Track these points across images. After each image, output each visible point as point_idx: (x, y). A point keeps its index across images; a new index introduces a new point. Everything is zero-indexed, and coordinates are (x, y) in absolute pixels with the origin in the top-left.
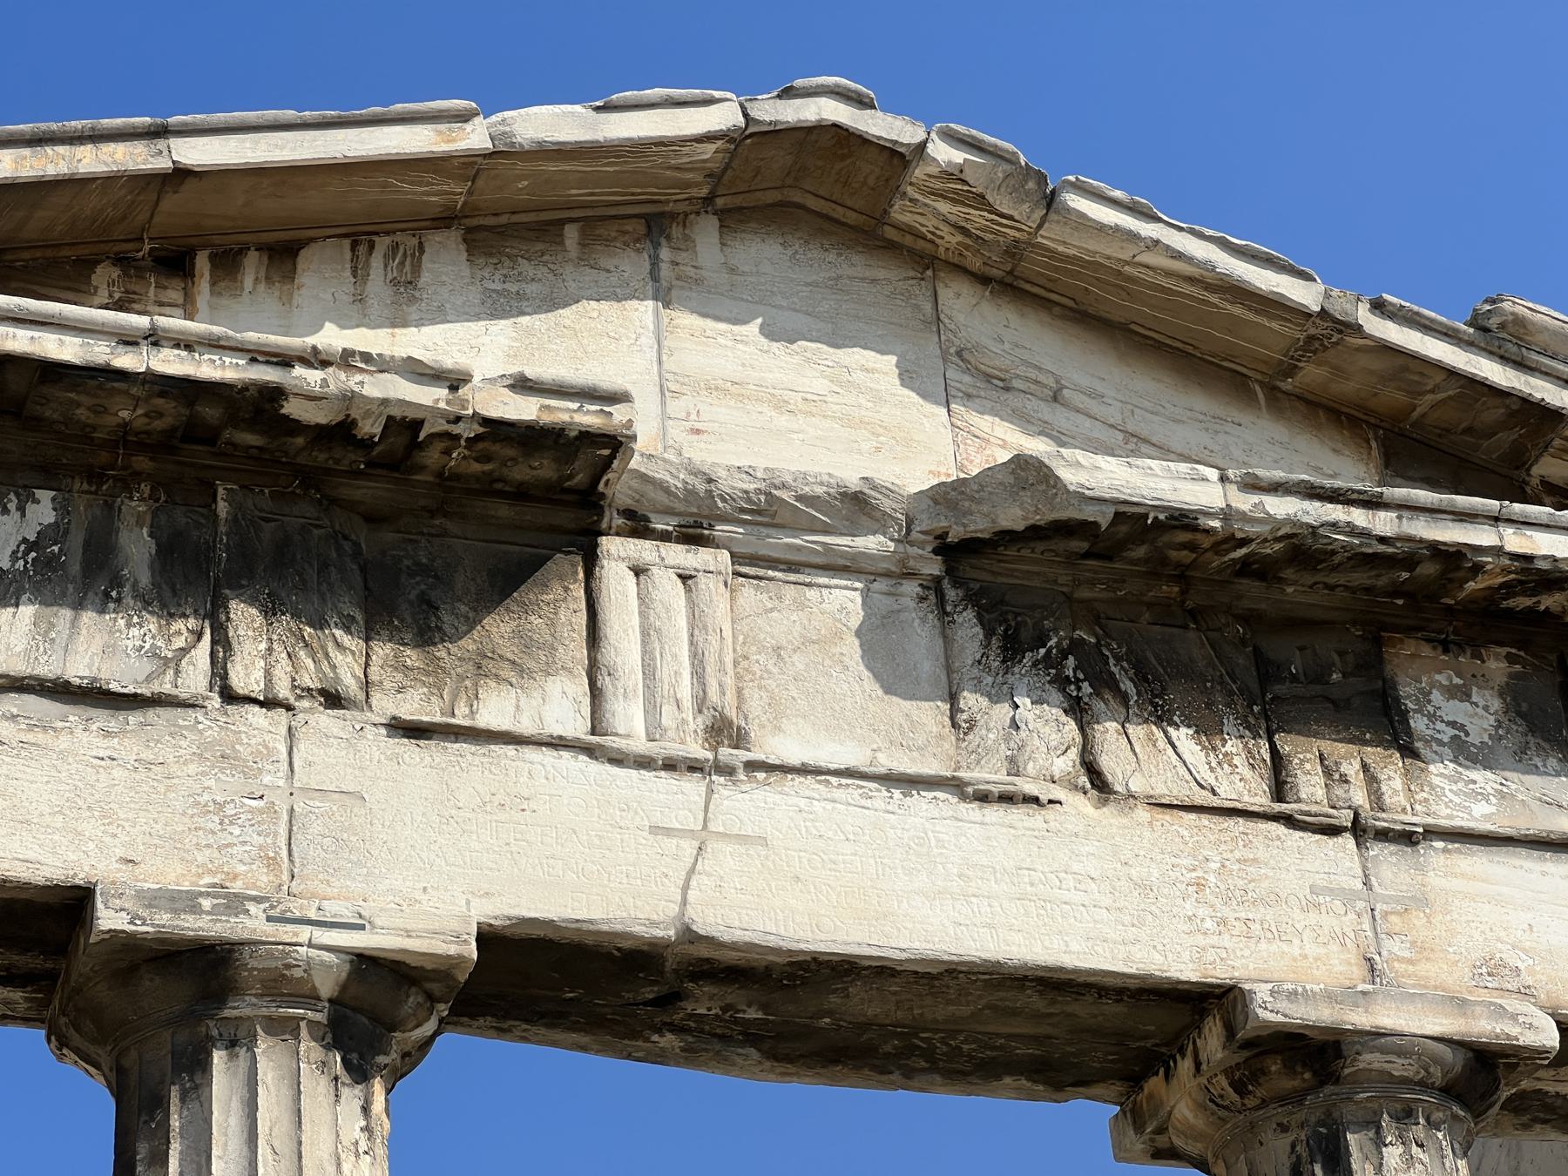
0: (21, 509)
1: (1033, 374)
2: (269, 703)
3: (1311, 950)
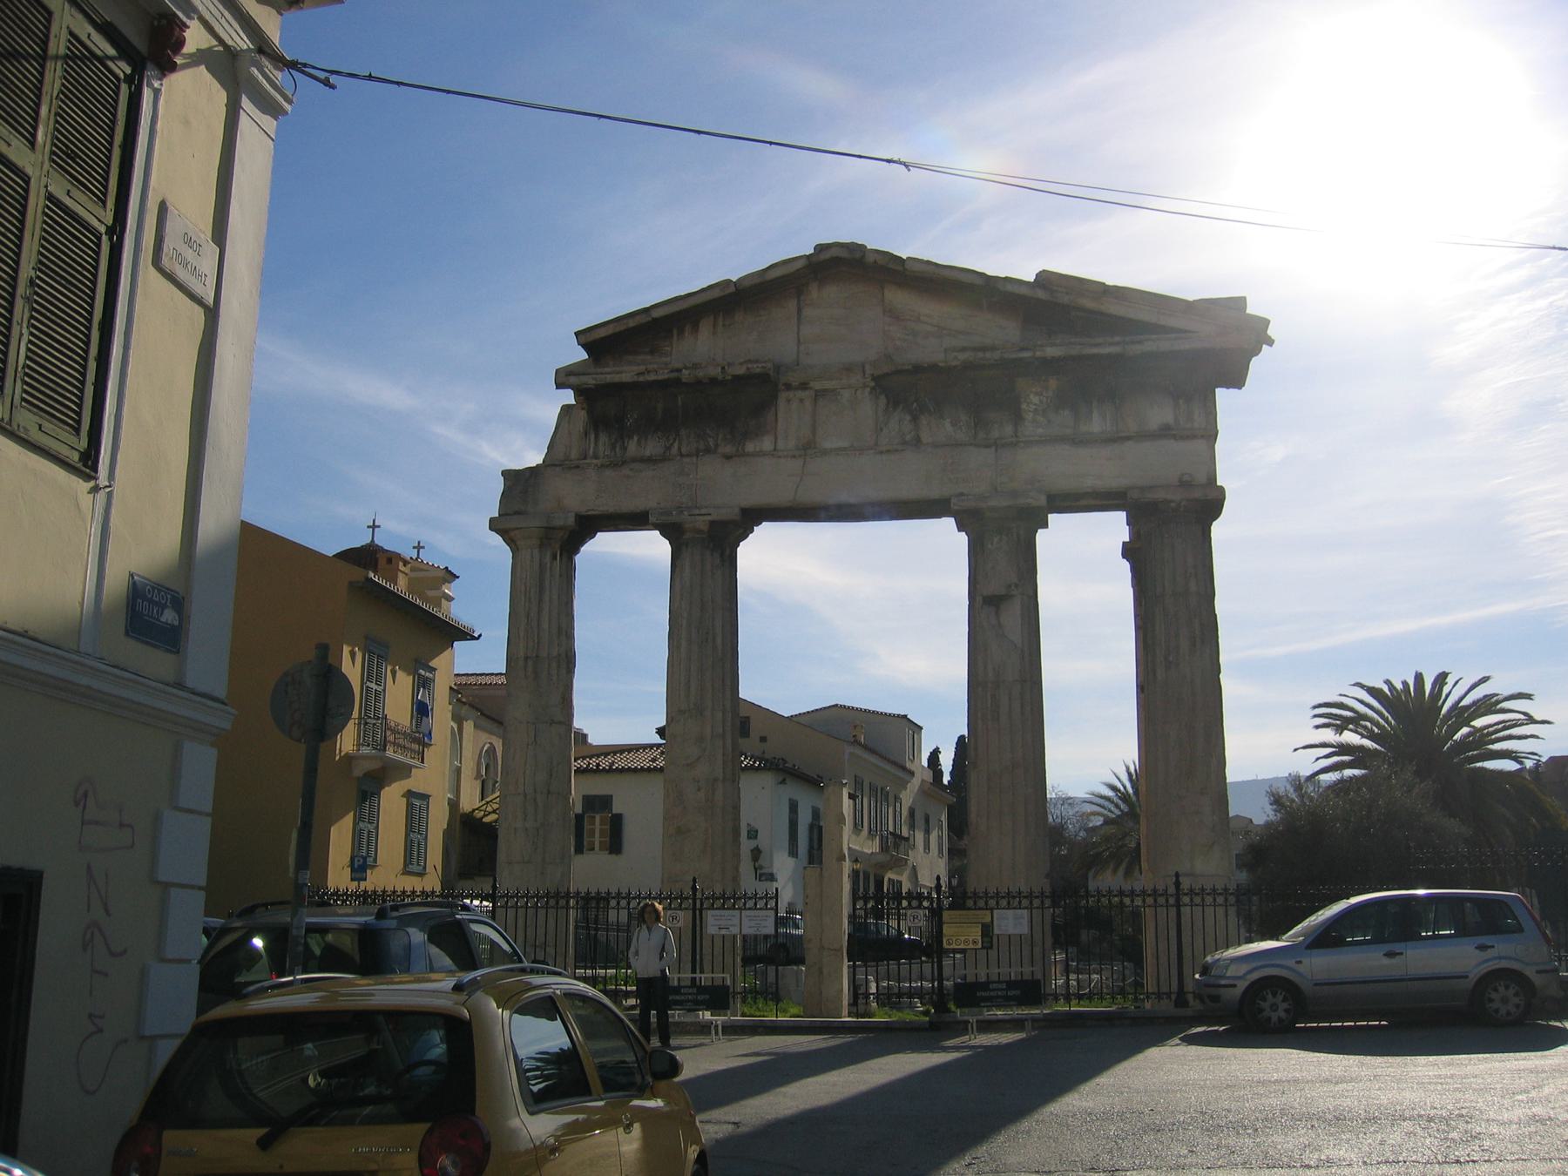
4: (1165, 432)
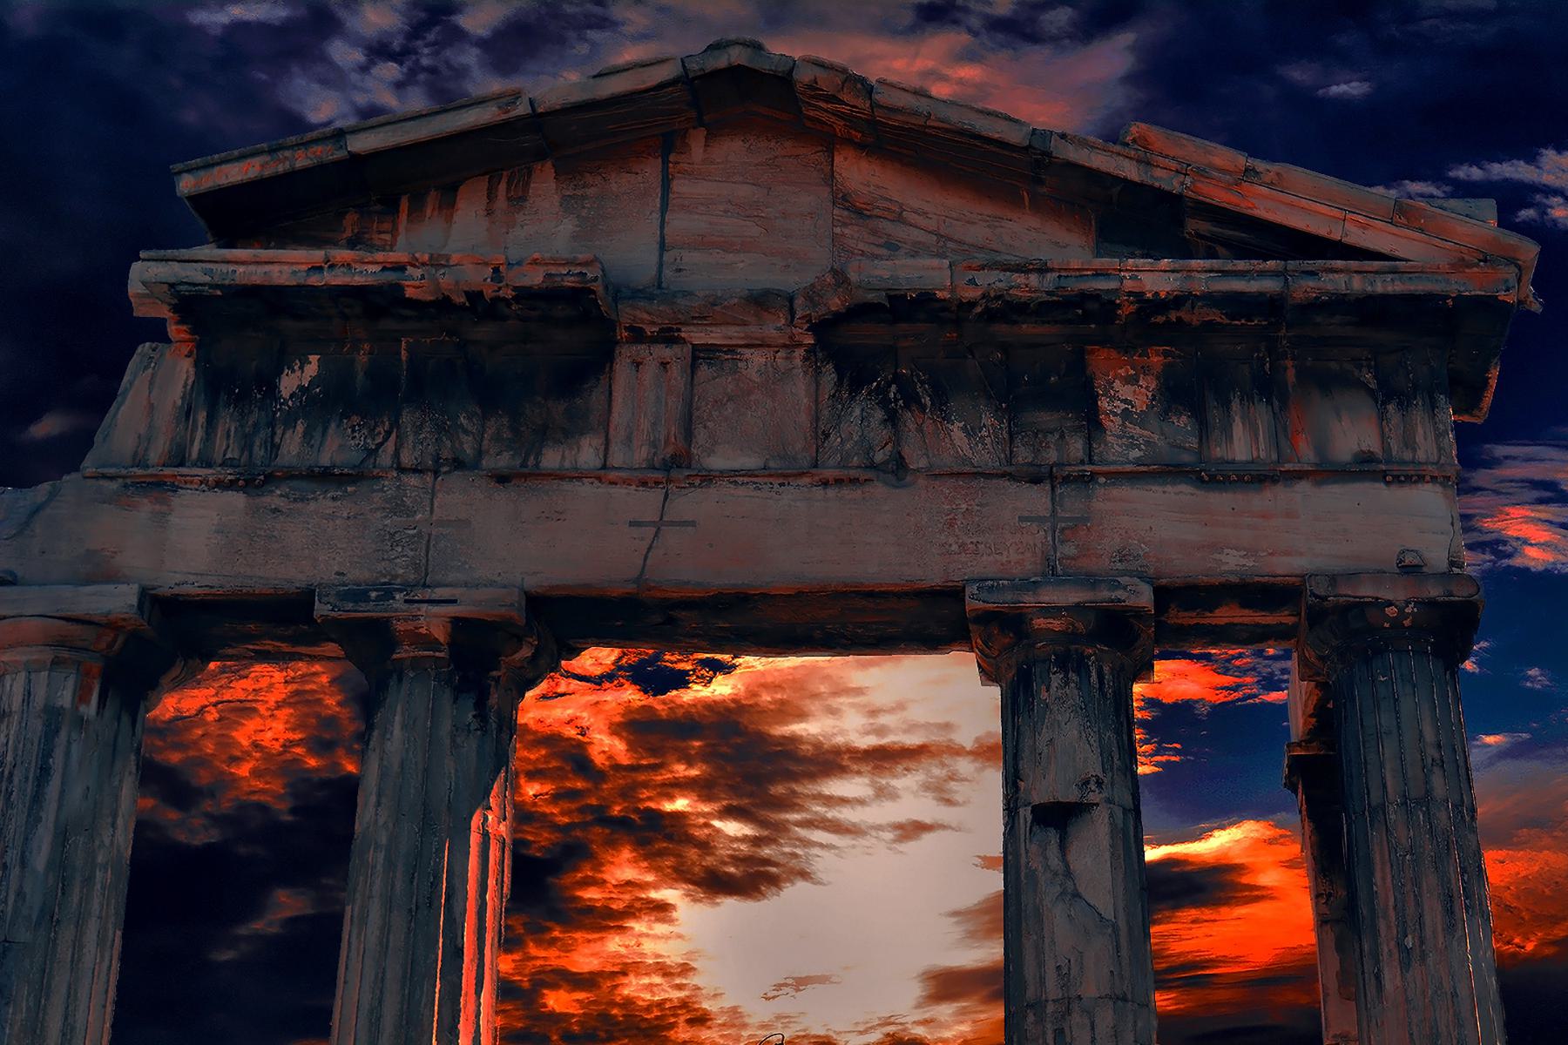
0: (301, 368)
1: (887, 204)
3: (1014, 557)
4: (1366, 468)
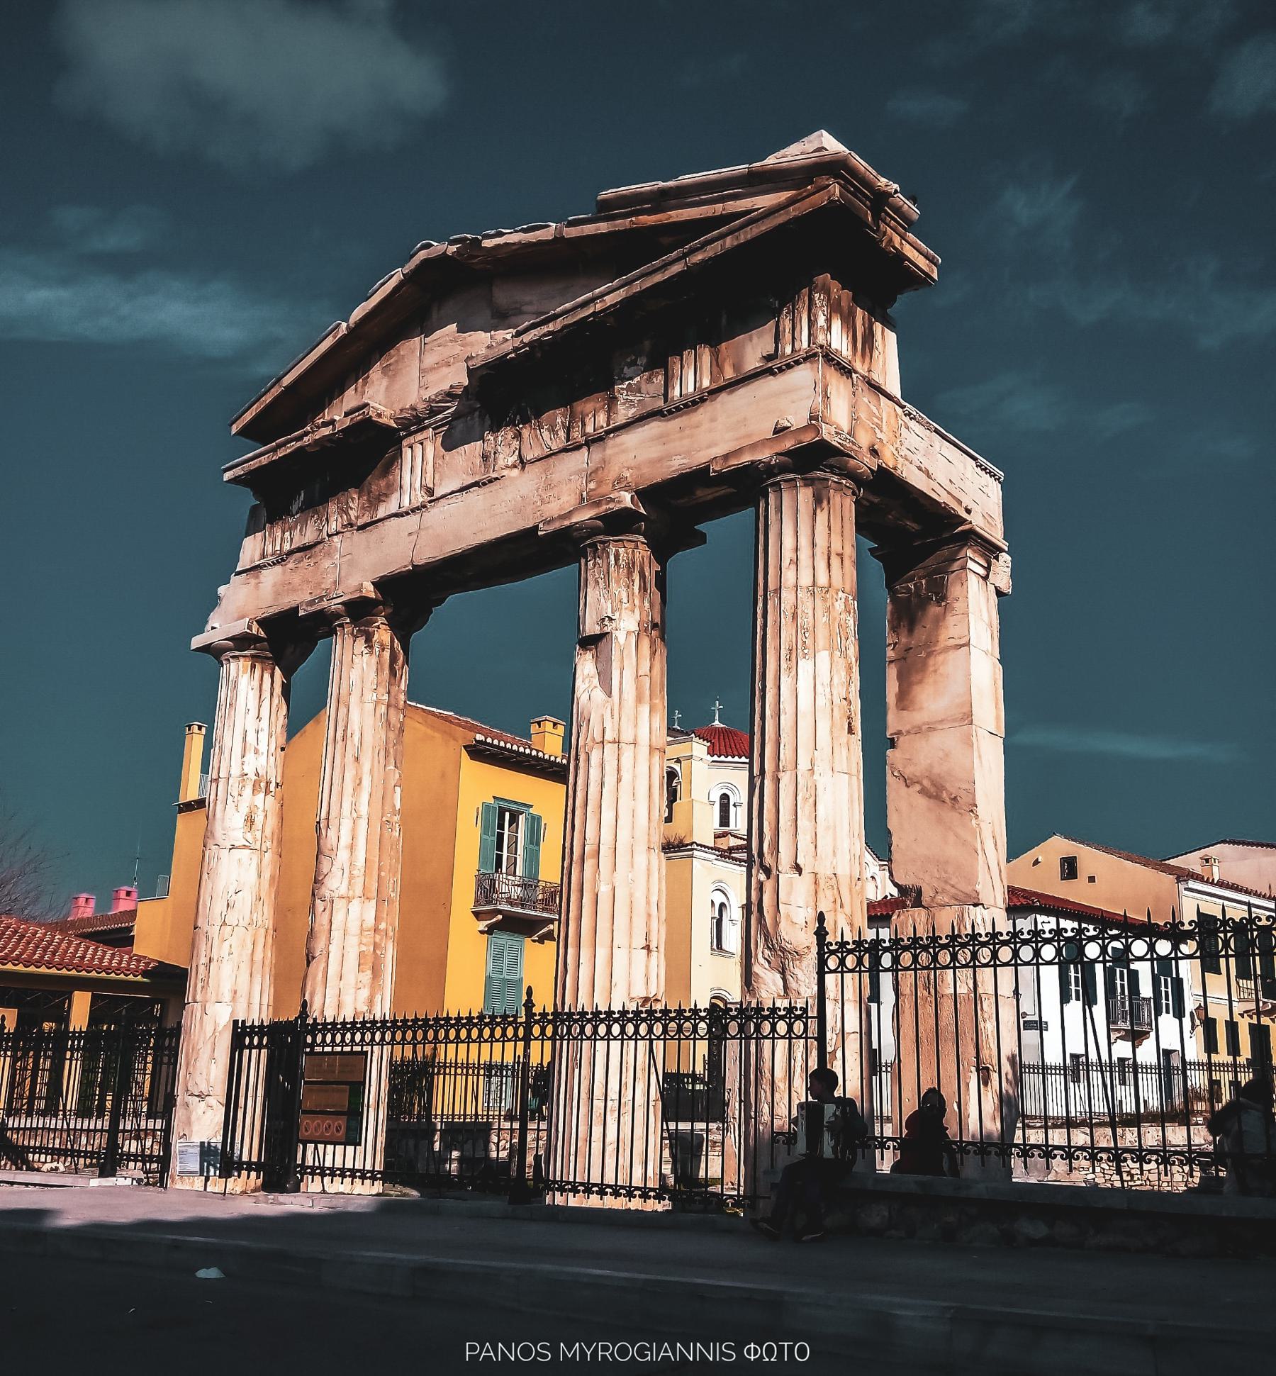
2: (337, 533)
